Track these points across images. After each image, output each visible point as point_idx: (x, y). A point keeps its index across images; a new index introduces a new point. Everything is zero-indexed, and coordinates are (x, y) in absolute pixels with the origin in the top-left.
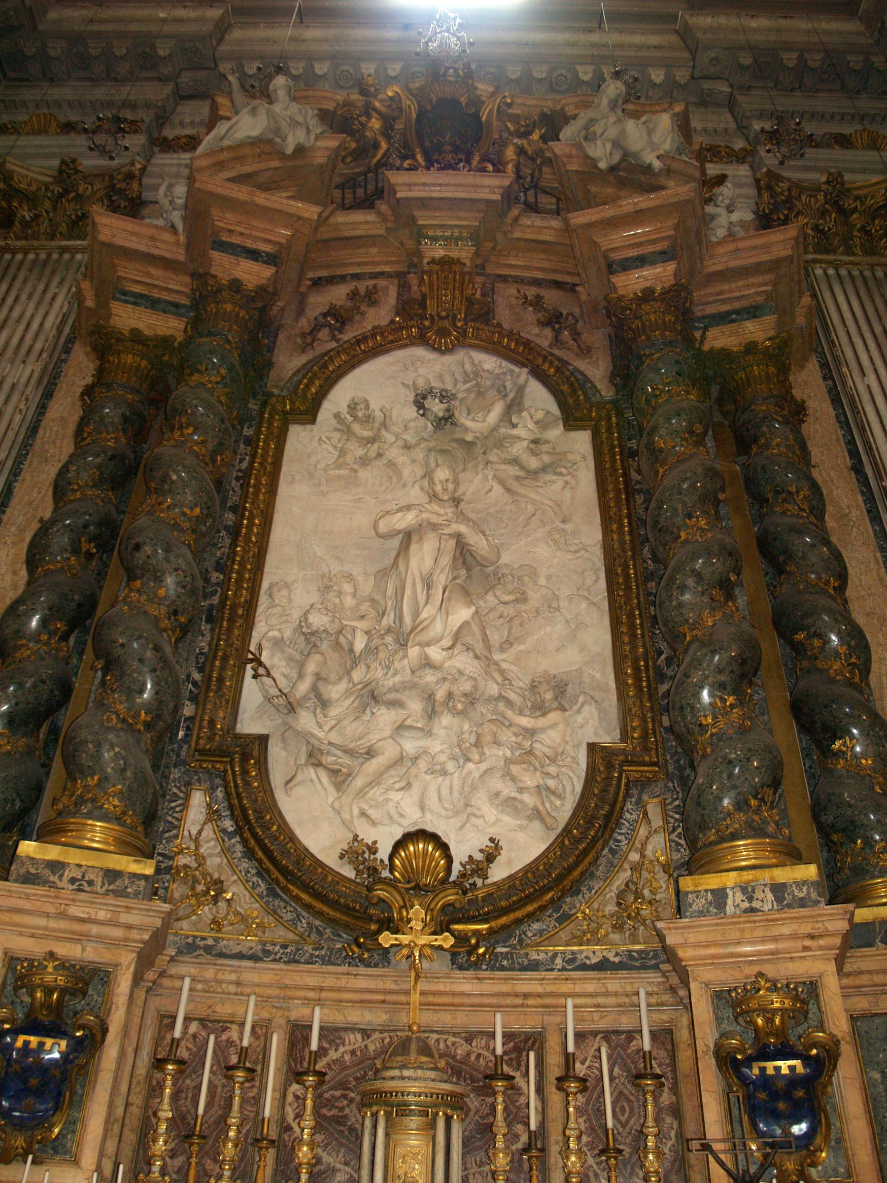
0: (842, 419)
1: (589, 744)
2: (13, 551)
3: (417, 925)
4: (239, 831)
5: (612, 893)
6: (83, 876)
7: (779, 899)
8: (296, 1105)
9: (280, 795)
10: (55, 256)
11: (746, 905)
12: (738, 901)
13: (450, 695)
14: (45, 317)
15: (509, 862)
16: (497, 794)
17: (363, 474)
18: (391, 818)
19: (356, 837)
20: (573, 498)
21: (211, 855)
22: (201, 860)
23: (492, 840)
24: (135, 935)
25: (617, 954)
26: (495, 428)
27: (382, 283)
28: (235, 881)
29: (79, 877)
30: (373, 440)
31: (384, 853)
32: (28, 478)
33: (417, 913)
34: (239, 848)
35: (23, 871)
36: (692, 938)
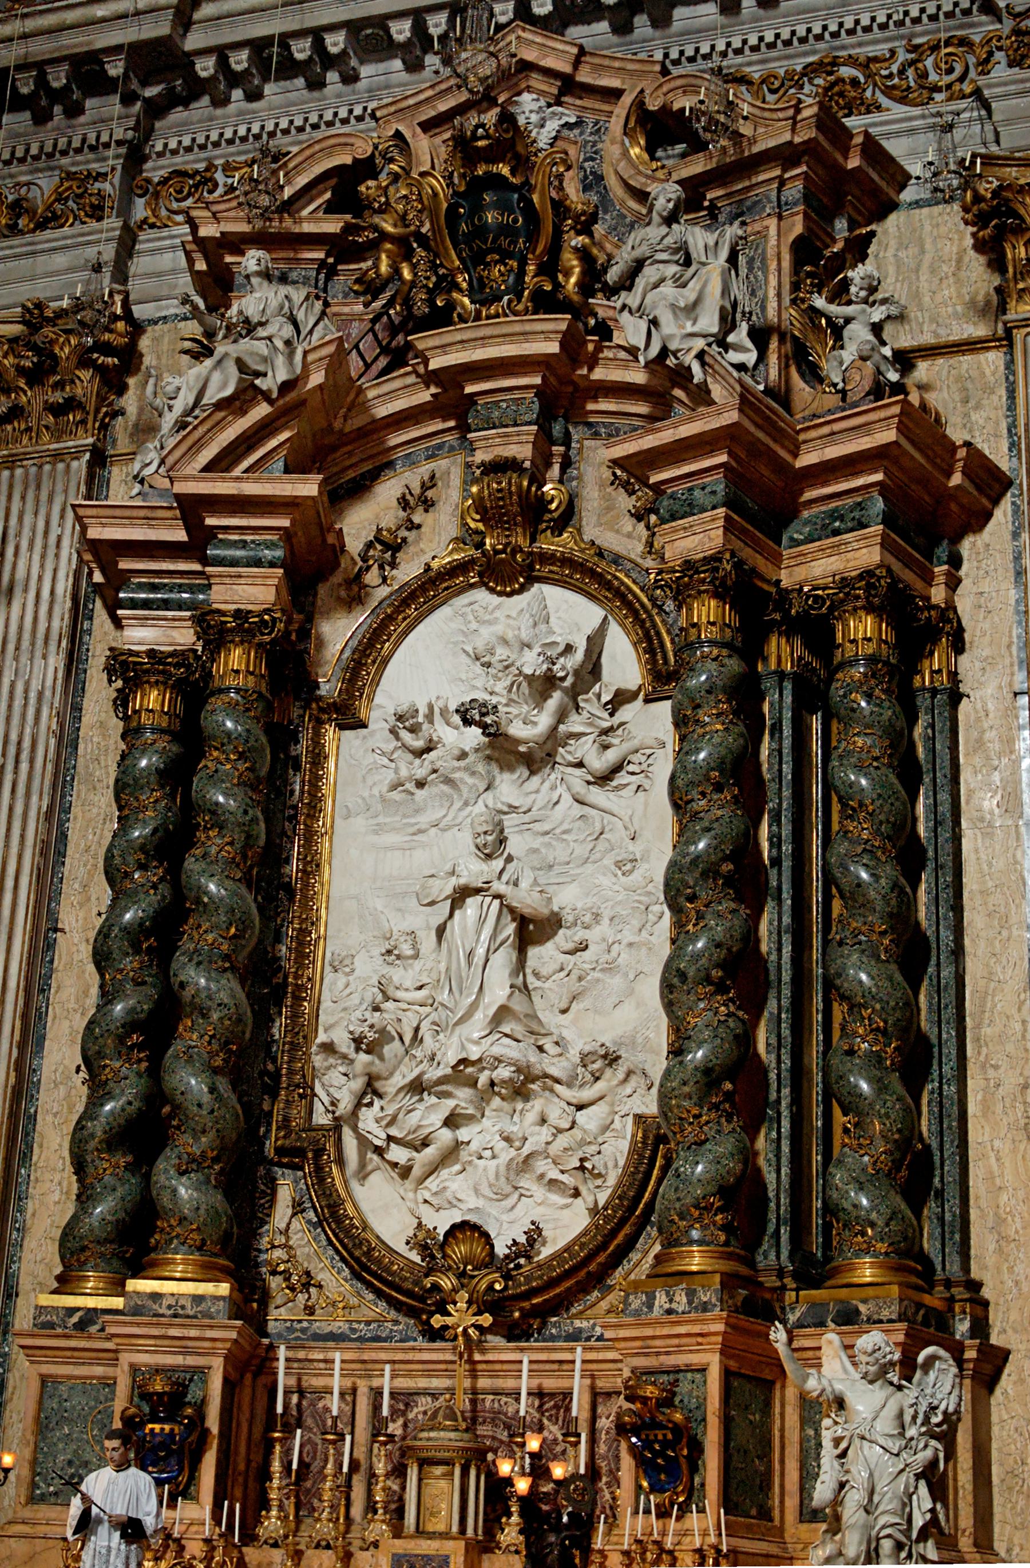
1: (636, 1116)
2: (81, 915)
3: (462, 1305)
7: (690, 1302)
9: (355, 1185)
10: (47, 468)
11: (667, 1306)
13: (492, 1084)
16: (542, 1176)
17: (420, 794)
20: (646, 804)
21: (300, 1246)
23: (533, 1223)
24: (219, 1345)
26: (554, 729)
27: (441, 464)
30: (428, 750)
32: (80, 814)
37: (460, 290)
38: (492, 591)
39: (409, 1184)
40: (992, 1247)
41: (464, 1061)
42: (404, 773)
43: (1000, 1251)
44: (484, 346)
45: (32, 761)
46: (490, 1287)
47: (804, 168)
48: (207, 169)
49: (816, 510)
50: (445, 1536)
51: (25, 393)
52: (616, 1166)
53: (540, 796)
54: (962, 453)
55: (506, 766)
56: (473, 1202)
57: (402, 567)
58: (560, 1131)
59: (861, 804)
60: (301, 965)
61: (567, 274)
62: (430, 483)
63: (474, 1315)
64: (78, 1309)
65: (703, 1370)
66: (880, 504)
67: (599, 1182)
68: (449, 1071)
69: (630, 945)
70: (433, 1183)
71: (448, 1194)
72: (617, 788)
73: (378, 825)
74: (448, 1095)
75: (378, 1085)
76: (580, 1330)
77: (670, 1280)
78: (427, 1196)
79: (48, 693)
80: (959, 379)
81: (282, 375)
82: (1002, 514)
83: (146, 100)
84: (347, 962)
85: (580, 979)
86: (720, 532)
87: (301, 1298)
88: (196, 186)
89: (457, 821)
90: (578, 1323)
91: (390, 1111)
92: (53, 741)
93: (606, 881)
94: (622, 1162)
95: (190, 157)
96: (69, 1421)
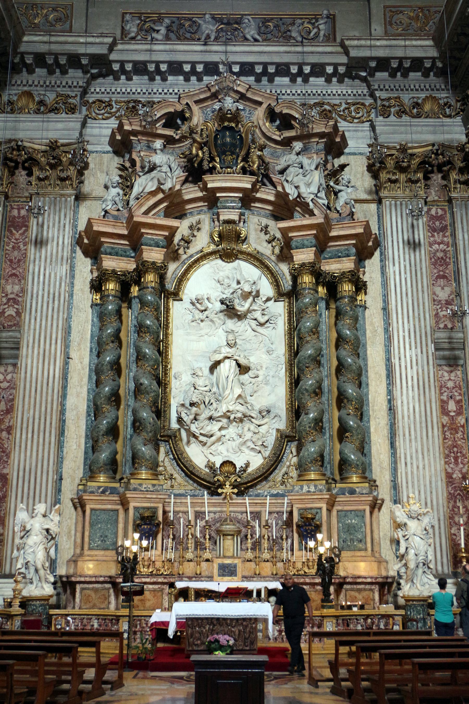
2: (78, 354)
4: (175, 458)
5: (281, 474)
7: (315, 489)
9: (186, 447)
10: (58, 199)
13: (235, 418)
14: (64, 239)
15: (252, 466)
16: (249, 447)
17: (202, 324)
19: (209, 461)
22: (165, 467)
27: (202, 217)
30: (205, 310)
31: (218, 465)
32: (75, 320)
33: (228, 483)
34: (175, 463)
36: (294, 497)
37: (216, 162)
38: (223, 261)
39: (205, 448)
40: (379, 470)
41: (228, 411)
42: (197, 317)
43: (381, 471)
44: (226, 182)
45: (59, 301)
46: (236, 480)
47: (325, 140)
48: (110, 101)
49: (332, 249)
50: (233, 557)
51: (49, 171)
53: (241, 328)
54: (373, 236)
55: (230, 317)
56: (225, 453)
57: (191, 249)
58: (255, 433)
59: (350, 341)
60: (166, 377)
61: (254, 163)
62: (199, 222)
64: (102, 487)
65: (320, 509)
66: (354, 250)
71: (218, 451)
74: (220, 421)
75: (197, 417)
76: (260, 493)
77: (309, 482)
79: (64, 278)
80: (363, 211)
81: (170, 186)
82: (377, 254)
83: (92, 74)
86: (313, 255)
87: (169, 482)
88: (106, 107)
90: (259, 491)
91: (202, 425)
92: (67, 295)
93: (264, 356)
94: (273, 443)
95: (103, 96)
96: (100, 523)
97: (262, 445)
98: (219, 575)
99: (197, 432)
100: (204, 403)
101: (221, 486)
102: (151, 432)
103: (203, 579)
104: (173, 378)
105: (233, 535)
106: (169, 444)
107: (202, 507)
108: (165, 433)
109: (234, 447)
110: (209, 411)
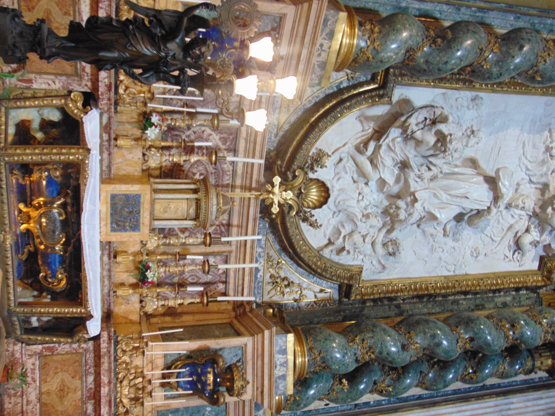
0: (514, 383)
6: (324, 51)
7: (279, 378)
8: (200, 131)
12: (280, 360)
13: (398, 208)
15: (308, 230)
18: (338, 174)
23: (321, 226)
25: (261, 276)
28: (313, 91)
29: (323, 49)
31: (320, 174)
33: (289, 195)
35: (330, 17)
41: (415, 200)
52: (340, 259)
58: (364, 237)
63: (279, 202)
67: (334, 252)
68: (412, 190)
69: (440, 258)
70: (350, 164)
72: (509, 246)
73: (536, 122)
74: (398, 180)
75: (412, 143)
78: (344, 161)
84: (475, 107)
85: (432, 235)
89: (521, 165)
91: (398, 150)
97: (343, 249)
98: (113, 197)
99: (385, 142)
100: (432, 155)
101: (286, 184)
102: (427, 62)
103: (105, 155)
104: (474, 94)
105: (196, 218)
106: (367, 83)
107: (246, 140)
108: (391, 78)
109: (347, 203)
110: (418, 163)
